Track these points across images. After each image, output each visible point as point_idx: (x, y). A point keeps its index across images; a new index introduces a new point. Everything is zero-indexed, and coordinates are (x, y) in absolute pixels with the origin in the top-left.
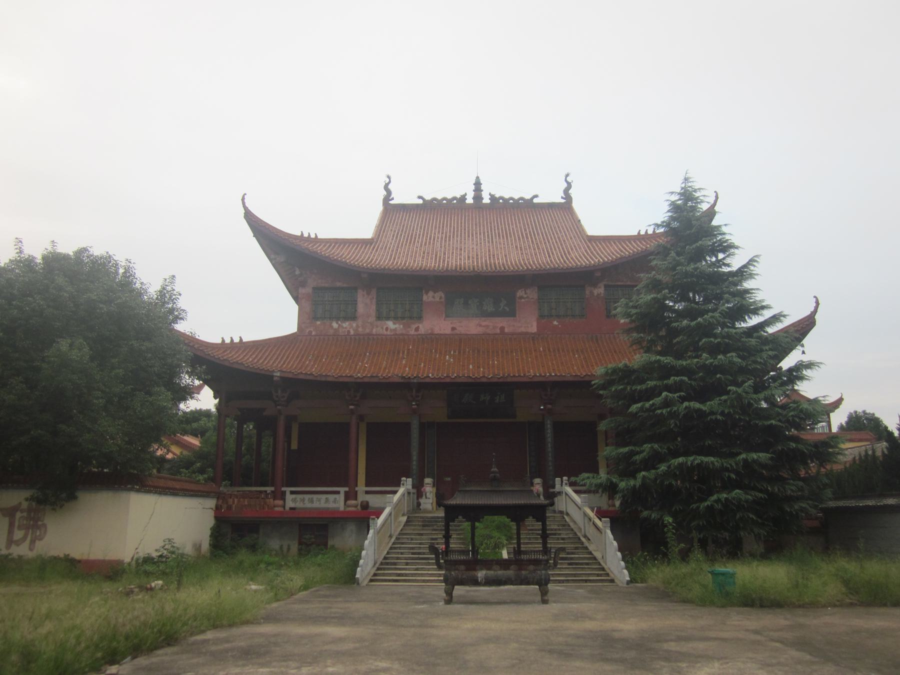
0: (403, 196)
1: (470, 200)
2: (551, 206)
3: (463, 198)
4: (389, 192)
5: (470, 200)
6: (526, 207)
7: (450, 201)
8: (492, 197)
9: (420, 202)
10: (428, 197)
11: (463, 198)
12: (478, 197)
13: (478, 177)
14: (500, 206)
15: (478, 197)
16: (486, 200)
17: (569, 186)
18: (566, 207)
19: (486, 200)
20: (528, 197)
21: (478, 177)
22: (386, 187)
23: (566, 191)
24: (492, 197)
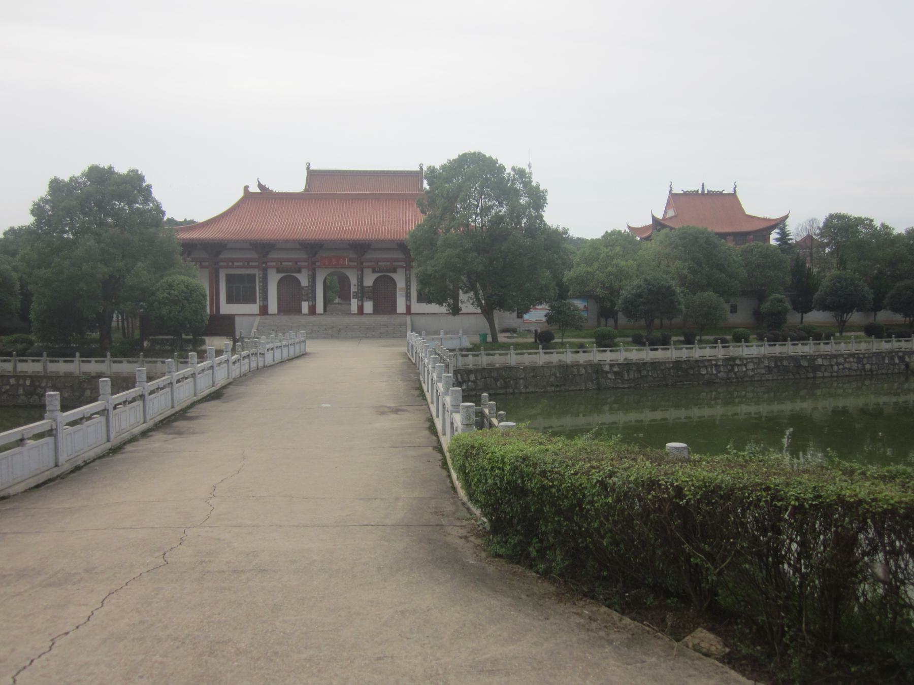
0: (677, 190)
1: (700, 192)
2: (729, 194)
3: (698, 191)
4: (671, 189)
5: (700, 192)
6: (720, 194)
7: (693, 192)
8: (708, 191)
9: (682, 192)
10: (685, 191)
11: (698, 191)
12: (703, 191)
13: (703, 184)
14: (711, 194)
15: (703, 191)
16: (706, 192)
17: (736, 186)
18: (734, 195)
19: (706, 192)
20: (721, 191)
21: (703, 184)
22: (670, 186)
23: (735, 189)
24: (708, 191)
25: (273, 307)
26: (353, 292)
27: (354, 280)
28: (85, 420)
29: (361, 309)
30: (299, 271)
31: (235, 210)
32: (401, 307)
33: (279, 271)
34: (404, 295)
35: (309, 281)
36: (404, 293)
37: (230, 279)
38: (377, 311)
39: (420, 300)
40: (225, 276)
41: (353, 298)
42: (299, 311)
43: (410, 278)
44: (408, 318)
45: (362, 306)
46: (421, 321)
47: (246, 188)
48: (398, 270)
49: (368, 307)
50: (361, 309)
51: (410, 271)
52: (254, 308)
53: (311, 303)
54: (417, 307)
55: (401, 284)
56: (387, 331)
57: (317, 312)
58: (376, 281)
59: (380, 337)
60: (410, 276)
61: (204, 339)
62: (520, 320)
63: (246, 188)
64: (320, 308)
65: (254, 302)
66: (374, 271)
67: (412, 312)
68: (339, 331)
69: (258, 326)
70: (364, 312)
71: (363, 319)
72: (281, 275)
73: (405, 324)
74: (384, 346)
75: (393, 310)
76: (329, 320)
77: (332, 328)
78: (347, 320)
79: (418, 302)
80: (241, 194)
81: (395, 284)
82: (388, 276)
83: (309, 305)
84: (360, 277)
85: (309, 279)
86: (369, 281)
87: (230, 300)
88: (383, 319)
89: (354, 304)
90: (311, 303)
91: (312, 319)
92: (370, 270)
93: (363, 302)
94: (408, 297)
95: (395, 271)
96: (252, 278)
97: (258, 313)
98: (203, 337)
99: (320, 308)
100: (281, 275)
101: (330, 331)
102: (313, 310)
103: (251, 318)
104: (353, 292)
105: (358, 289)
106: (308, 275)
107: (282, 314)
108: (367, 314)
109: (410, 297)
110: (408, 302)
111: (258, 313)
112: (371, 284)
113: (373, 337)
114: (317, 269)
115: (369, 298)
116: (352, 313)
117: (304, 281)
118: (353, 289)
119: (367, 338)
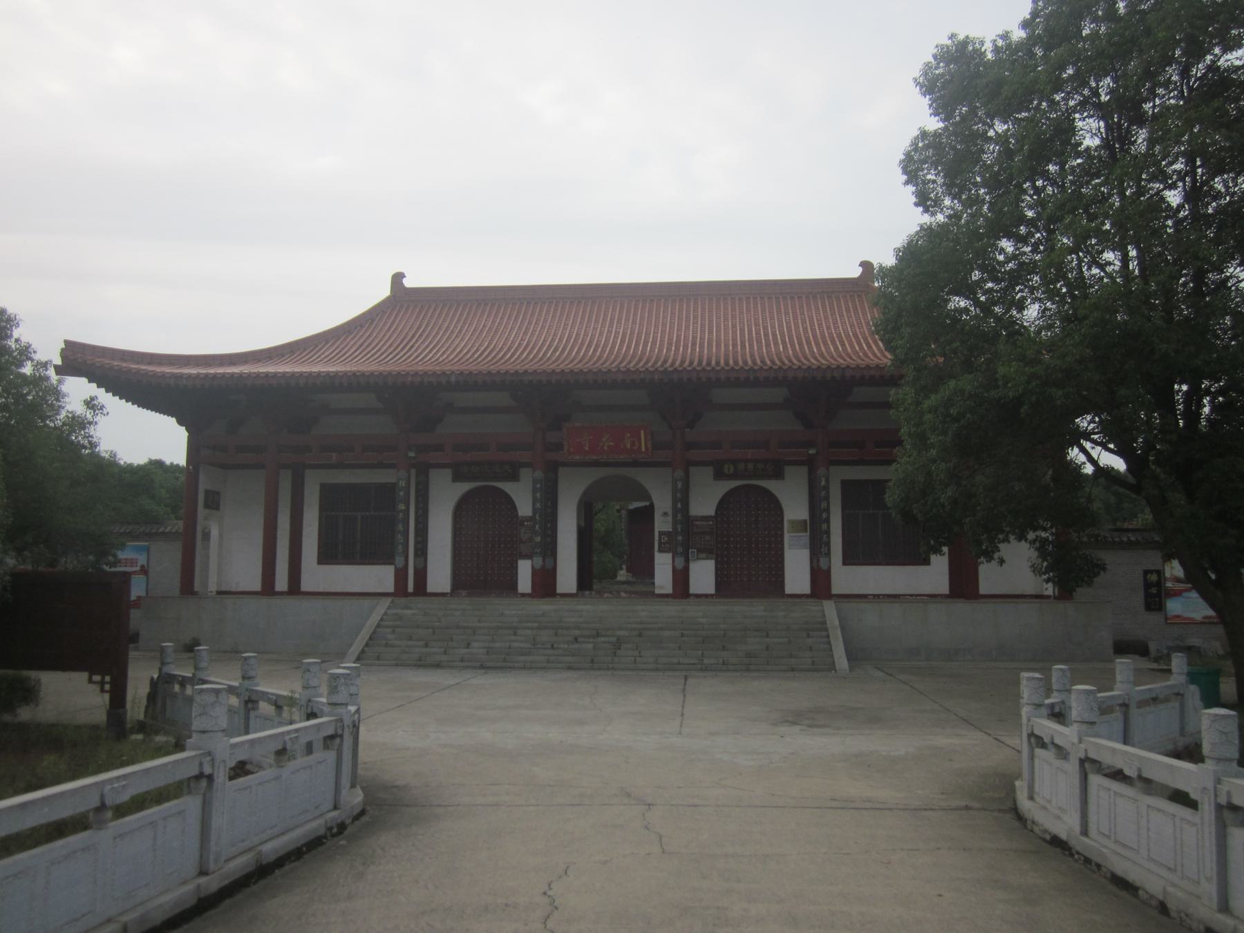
25: (440, 576)
26: (661, 533)
27: (663, 503)
28: (109, 814)
29: (681, 579)
30: (514, 477)
31: (362, 326)
32: (797, 576)
33: (458, 477)
34: (807, 541)
35: (535, 501)
36: (805, 537)
37: (331, 498)
38: (725, 586)
39: (848, 560)
40: (318, 488)
41: (661, 551)
42: (509, 586)
43: (826, 488)
44: (829, 608)
45: (686, 571)
46: (869, 617)
47: (398, 278)
48: (789, 470)
49: (703, 575)
50: (681, 579)
51: (828, 470)
52: (380, 577)
53: (538, 561)
54: (846, 578)
55: (795, 509)
56: (767, 648)
57: (560, 590)
58: (723, 504)
59: (748, 670)
60: (827, 481)
61: (38, 681)
62: (1154, 618)
63: (398, 278)
64: (567, 577)
65: (387, 560)
66: (719, 475)
67: (835, 591)
68: (618, 645)
69: (378, 626)
70: (692, 590)
71: (692, 611)
72: (465, 487)
73: (823, 626)
74: (795, 718)
75: (773, 583)
76: (592, 609)
77: (598, 635)
78: (643, 611)
79: (844, 563)
80: (384, 292)
81: (778, 509)
82: (758, 487)
83: (533, 567)
84: (679, 485)
85: (534, 490)
86: (704, 504)
87: (327, 556)
88: (751, 610)
89: (663, 566)
90: (538, 561)
91: (544, 606)
92: (709, 471)
93: (687, 561)
94: (818, 547)
95: (778, 474)
96: (387, 493)
97: (391, 590)
98: (33, 674)
99: (567, 577)
100: (465, 487)
101: (590, 646)
102: (545, 584)
103: (366, 603)
104: (661, 533)
105: (675, 523)
106: (535, 482)
107: (464, 593)
108: (698, 596)
109: (828, 544)
110: (823, 563)
111: (391, 590)
112: (710, 510)
113: (724, 667)
114: (562, 471)
115: (705, 552)
116: (657, 591)
117: (525, 508)
118: (662, 524)
119: (706, 669)
